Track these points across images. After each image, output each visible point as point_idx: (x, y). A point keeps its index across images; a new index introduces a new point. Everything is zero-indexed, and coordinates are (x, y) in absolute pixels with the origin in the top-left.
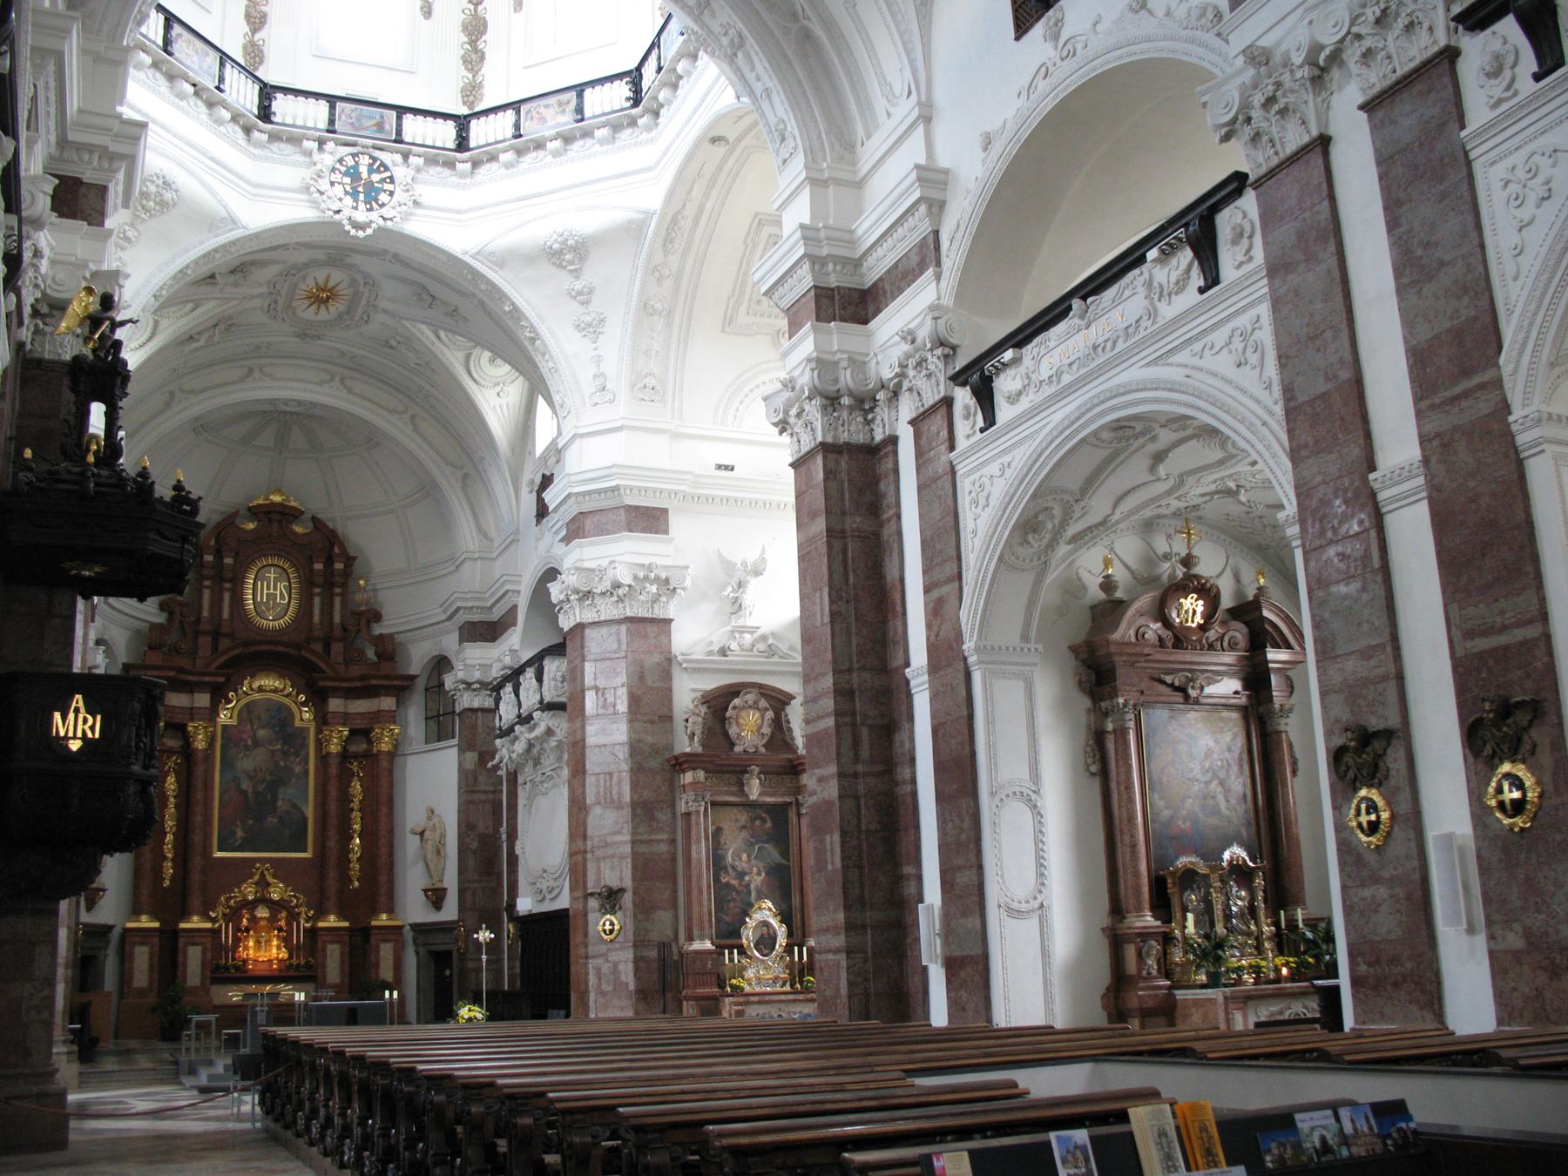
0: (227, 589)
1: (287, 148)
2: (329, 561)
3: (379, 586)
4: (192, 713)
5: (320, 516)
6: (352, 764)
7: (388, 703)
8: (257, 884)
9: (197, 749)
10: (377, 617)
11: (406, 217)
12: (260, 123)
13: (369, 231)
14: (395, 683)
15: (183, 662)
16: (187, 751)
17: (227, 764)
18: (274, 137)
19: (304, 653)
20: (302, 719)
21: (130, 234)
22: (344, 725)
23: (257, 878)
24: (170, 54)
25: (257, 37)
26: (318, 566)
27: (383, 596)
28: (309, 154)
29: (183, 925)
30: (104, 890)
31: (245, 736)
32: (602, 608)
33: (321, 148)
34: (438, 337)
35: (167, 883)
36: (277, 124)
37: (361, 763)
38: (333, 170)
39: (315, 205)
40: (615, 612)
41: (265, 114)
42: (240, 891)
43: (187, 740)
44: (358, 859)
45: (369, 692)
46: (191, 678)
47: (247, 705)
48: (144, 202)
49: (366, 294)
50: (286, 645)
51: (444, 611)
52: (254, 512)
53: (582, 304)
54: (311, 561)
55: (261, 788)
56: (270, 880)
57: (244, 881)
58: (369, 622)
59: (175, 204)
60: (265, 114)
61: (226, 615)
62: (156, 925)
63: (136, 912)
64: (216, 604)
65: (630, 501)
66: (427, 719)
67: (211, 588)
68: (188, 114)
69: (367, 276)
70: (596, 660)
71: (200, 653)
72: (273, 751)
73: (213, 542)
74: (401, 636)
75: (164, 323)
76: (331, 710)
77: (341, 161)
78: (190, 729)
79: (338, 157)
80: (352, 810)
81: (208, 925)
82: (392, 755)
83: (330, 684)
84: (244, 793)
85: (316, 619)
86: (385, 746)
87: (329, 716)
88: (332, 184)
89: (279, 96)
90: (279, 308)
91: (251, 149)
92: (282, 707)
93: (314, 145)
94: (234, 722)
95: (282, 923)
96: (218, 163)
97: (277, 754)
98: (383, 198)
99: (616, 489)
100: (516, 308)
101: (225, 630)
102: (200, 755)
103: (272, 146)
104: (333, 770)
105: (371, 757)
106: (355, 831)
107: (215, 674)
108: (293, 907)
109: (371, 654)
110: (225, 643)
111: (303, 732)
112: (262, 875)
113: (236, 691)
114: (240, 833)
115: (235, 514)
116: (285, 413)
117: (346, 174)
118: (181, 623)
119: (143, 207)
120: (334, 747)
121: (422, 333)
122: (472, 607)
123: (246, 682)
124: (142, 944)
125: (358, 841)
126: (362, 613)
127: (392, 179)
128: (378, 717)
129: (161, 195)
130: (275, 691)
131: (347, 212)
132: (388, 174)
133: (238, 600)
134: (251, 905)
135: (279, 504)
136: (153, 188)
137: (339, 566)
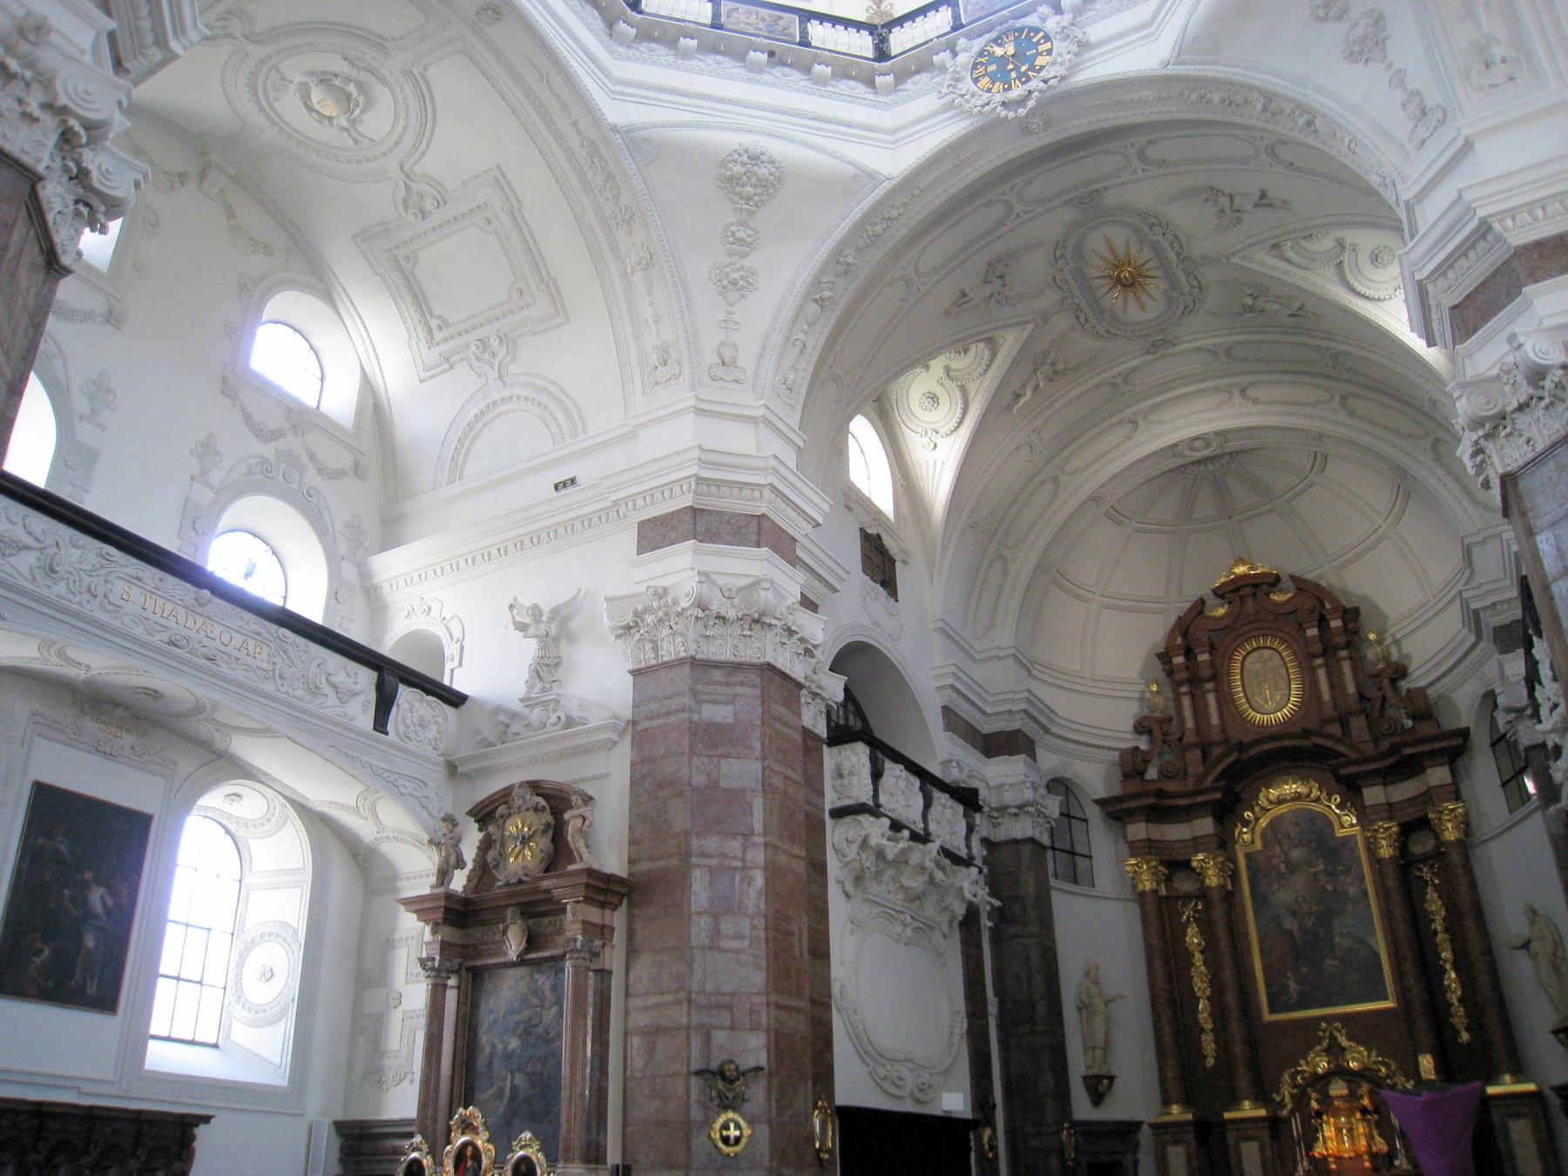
0: (1209, 691)
1: (923, 78)
2: (1323, 621)
3: (1399, 635)
4: (1196, 843)
5: (1309, 577)
6: (1420, 870)
7: (1438, 775)
8: (1327, 1051)
9: (1210, 887)
10: (1400, 672)
11: (1073, 69)
12: (876, 64)
13: (1031, 103)
14: (1438, 745)
15: (1171, 786)
16: (1204, 894)
17: (1260, 901)
18: (902, 76)
19: (1316, 740)
20: (1343, 827)
21: (740, 234)
22: (1391, 819)
23: (1325, 1043)
24: (720, 27)
25: (883, 7)
26: (1312, 632)
27: (1407, 646)
28: (943, 69)
29: (1227, 1115)
30: (1111, 1079)
31: (1275, 862)
32: (1534, 432)
33: (955, 54)
34: (1287, 260)
35: (1210, 1062)
36: (895, 57)
37: (1432, 866)
38: (975, 67)
39: (970, 114)
40: (1557, 426)
41: (882, 54)
42: (1307, 1063)
43: (1200, 875)
44: (1460, 1000)
45: (1408, 767)
46: (1181, 802)
47: (1271, 823)
48: (738, 190)
49: (1166, 245)
50: (1291, 736)
51: (1470, 630)
52: (1219, 593)
53: (1340, 18)
54: (1301, 628)
55: (1309, 923)
56: (1344, 1042)
57: (1311, 1048)
58: (1393, 681)
59: (779, 180)
60: (882, 54)
61: (1215, 720)
62: (1189, 1117)
63: (1166, 1103)
64: (1200, 712)
65: (1518, 238)
66: (1504, 785)
67: (1193, 696)
68: (774, 85)
69: (1144, 215)
70: (1552, 525)
71: (1191, 771)
72: (1314, 874)
73: (1179, 641)
74: (1438, 686)
75: (972, 388)
76: (1368, 802)
77: (981, 54)
78: (1195, 864)
79: (976, 49)
80: (1435, 932)
81: (1262, 1112)
82: (1466, 843)
83: (1354, 769)
84: (1290, 933)
85: (1326, 695)
86: (1450, 833)
87: (1368, 811)
88: (976, 81)
89: (896, 30)
90: (1091, 317)
91: (881, 99)
92: (1313, 817)
93: (945, 56)
94: (1258, 845)
95: (1366, 1102)
96: (828, 121)
97: (1321, 877)
98: (1040, 61)
99: (1484, 229)
100: (1269, 97)
101: (1216, 736)
102: (1215, 896)
103: (905, 86)
104: (1392, 881)
105: (1439, 854)
106: (1445, 961)
107: (1205, 791)
108: (1384, 1079)
109: (1409, 723)
110: (1217, 751)
111: (1348, 840)
112: (1332, 1038)
113: (1252, 810)
114: (1293, 986)
115: (1202, 601)
116: (1199, 462)
117: (986, 65)
118: (1164, 742)
119: (740, 195)
120: (1386, 851)
121: (1266, 265)
122: (1494, 605)
123: (1261, 796)
124: (1176, 1143)
125: (1453, 975)
126: (1378, 674)
127: (1047, 38)
128: (1427, 798)
129: (755, 174)
130: (1298, 797)
131: (998, 98)
132: (1041, 34)
133: (1226, 701)
134: (1320, 1081)
135: (1244, 576)
136: (738, 169)
137: (1336, 623)
